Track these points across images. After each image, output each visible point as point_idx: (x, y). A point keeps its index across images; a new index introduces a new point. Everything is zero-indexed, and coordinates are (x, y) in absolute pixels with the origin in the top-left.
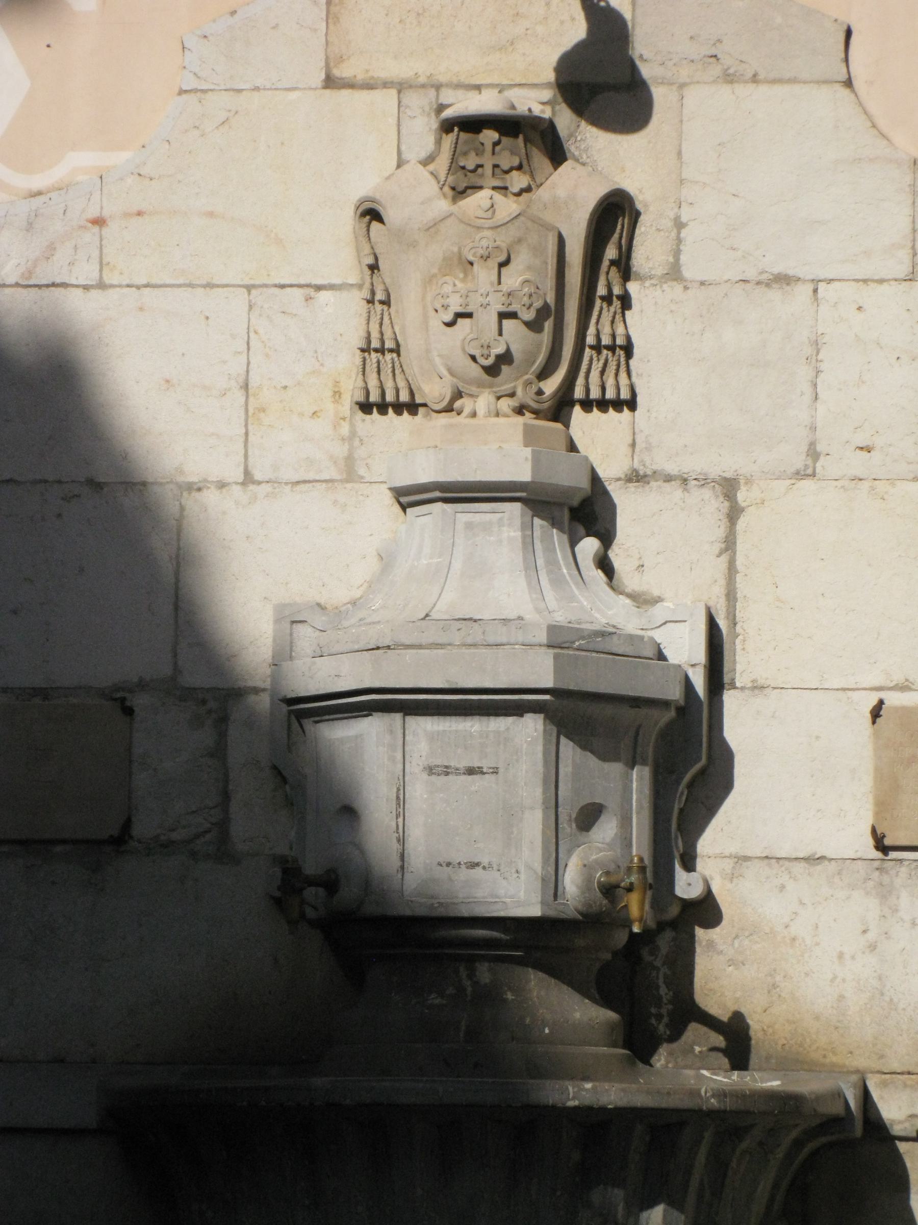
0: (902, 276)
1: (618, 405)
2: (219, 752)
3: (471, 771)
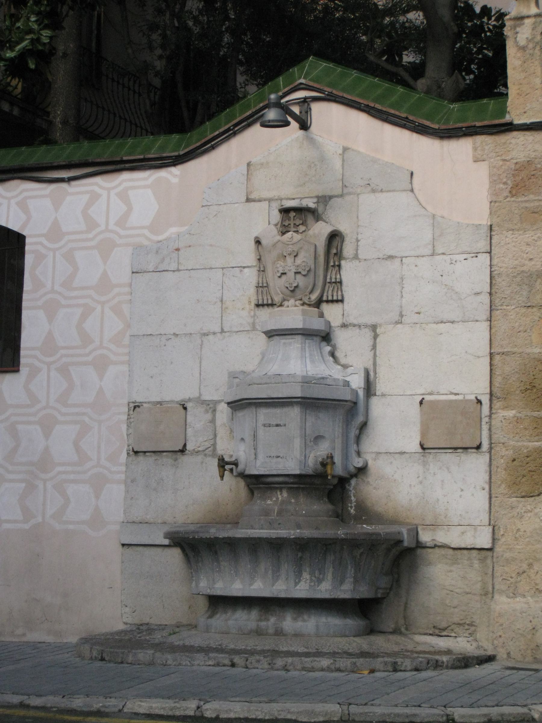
0: (430, 254)
1: (337, 301)
2: (213, 421)
3: (277, 425)
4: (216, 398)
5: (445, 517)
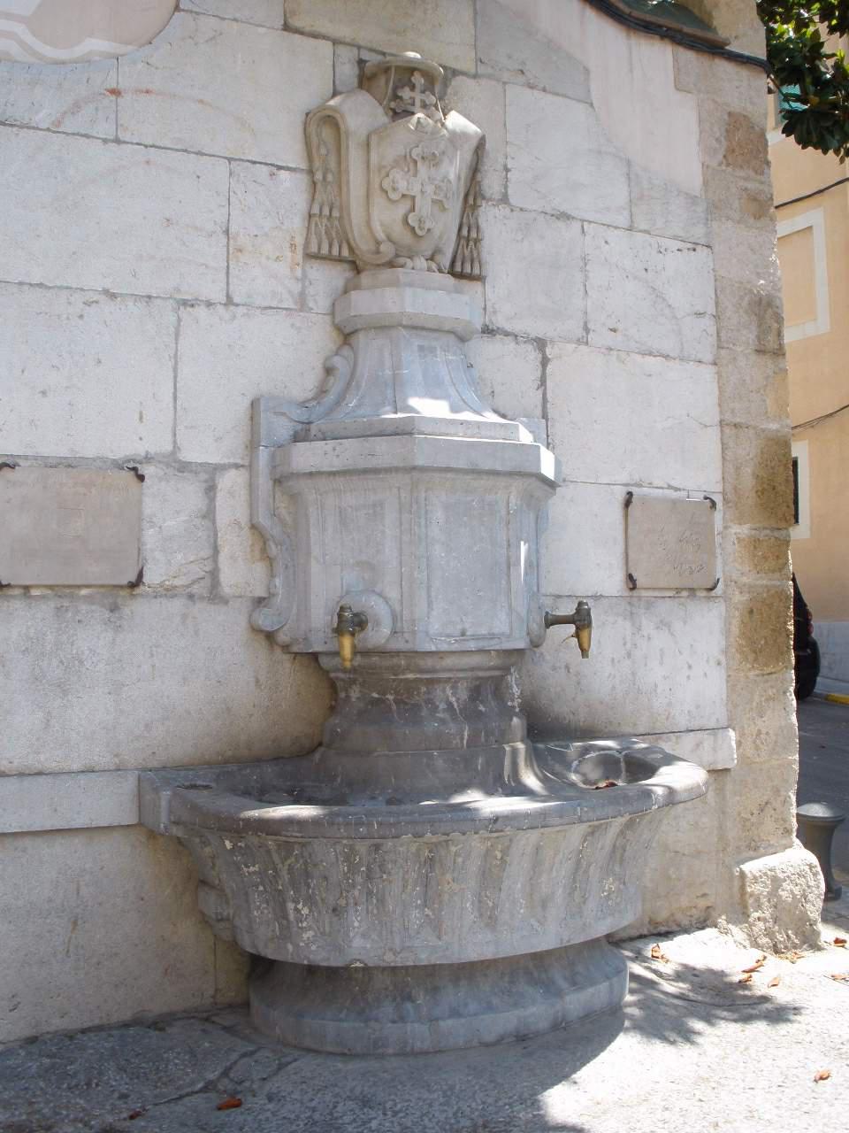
2: (209, 514)
4: (215, 459)
5: (667, 719)
